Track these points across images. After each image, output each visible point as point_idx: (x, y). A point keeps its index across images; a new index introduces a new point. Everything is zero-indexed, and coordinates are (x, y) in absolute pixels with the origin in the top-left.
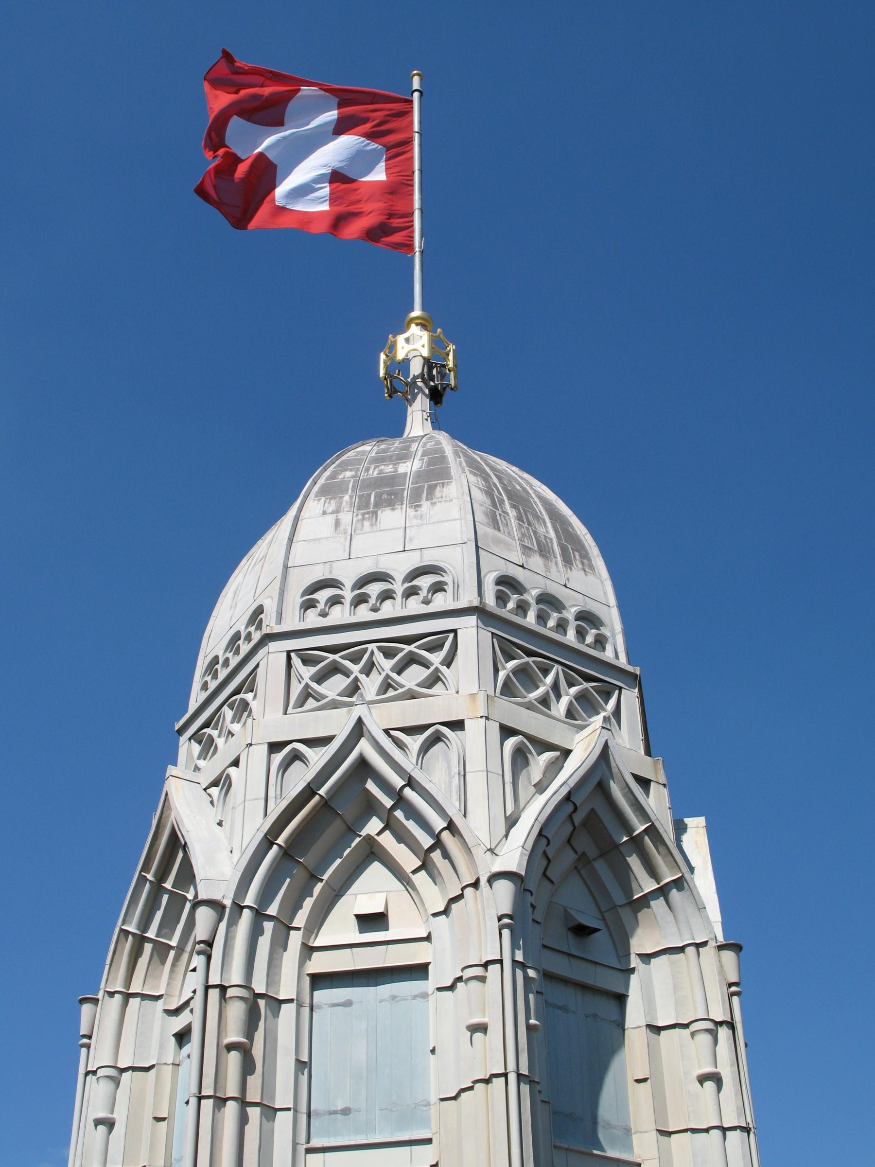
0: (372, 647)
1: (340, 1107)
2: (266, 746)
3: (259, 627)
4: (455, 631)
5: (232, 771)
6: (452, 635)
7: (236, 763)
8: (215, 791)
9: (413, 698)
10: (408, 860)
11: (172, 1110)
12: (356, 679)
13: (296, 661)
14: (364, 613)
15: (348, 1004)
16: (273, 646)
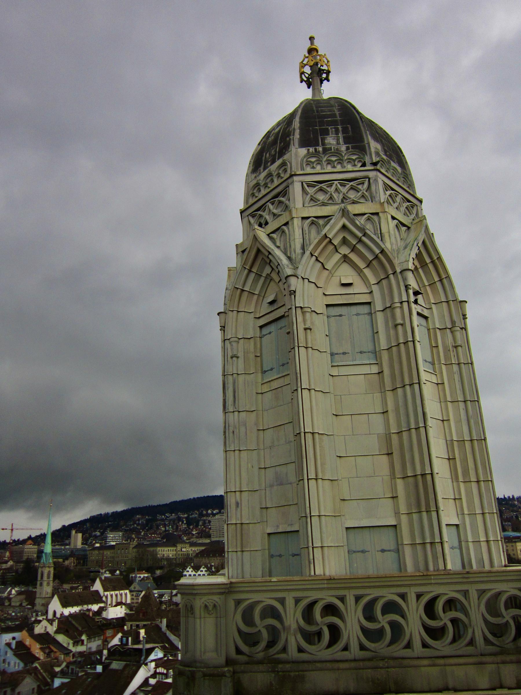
0: (336, 182)
1: (341, 351)
2: (300, 219)
3: (285, 171)
4: (369, 179)
5: (285, 228)
6: (367, 179)
7: (286, 224)
8: (274, 236)
9: (353, 203)
10: (361, 265)
11: (261, 354)
12: (331, 194)
13: (305, 186)
14: (329, 169)
15: (340, 316)
16: (295, 178)
